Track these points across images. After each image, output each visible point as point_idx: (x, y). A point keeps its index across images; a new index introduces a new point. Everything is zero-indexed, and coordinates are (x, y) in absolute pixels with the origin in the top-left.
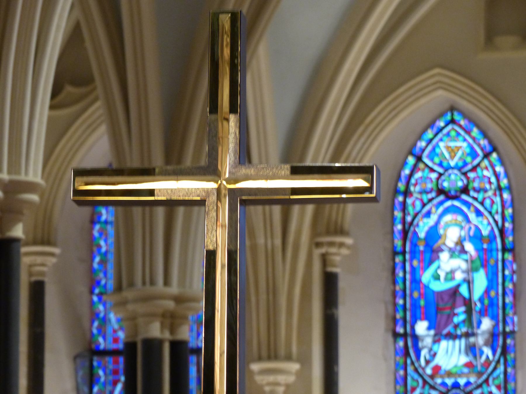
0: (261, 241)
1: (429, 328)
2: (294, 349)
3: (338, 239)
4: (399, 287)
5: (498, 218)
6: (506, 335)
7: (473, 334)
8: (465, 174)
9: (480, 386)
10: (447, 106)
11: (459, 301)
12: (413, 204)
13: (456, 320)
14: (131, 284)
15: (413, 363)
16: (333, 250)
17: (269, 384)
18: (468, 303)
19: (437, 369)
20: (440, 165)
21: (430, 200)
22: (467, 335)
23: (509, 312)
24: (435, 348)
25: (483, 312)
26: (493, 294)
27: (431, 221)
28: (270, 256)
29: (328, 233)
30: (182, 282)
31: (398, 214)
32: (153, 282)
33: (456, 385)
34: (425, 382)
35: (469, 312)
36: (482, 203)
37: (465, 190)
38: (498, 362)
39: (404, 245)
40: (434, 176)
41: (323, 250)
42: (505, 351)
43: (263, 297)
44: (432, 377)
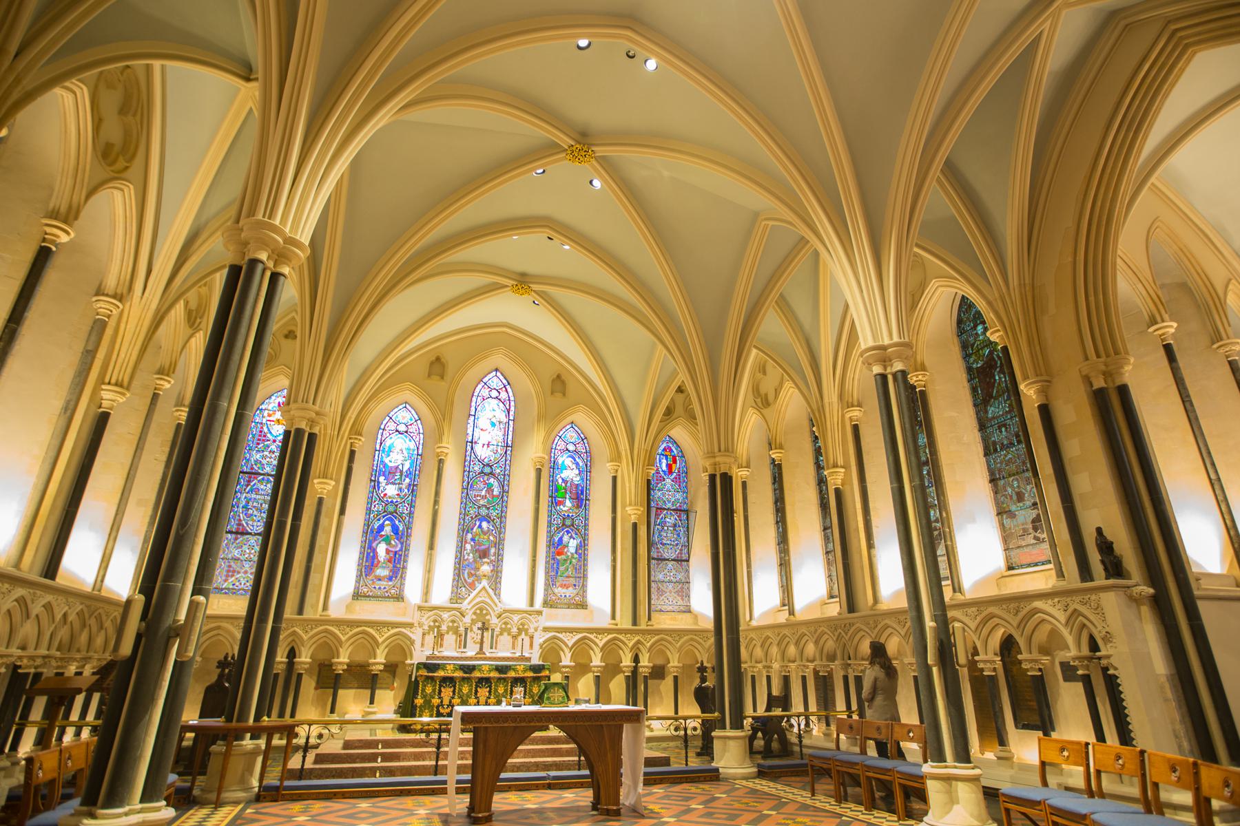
0: (329, 431)
3: (359, 437)
4: (375, 463)
6: (414, 485)
14: (296, 401)
18: (401, 472)
19: (385, 495)
23: (417, 477)
25: (407, 476)
29: (355, 434)
30: (321, 407)
33: (392, 502)
35: (401, 475)
37: (406, 432)
42: (413, 491)
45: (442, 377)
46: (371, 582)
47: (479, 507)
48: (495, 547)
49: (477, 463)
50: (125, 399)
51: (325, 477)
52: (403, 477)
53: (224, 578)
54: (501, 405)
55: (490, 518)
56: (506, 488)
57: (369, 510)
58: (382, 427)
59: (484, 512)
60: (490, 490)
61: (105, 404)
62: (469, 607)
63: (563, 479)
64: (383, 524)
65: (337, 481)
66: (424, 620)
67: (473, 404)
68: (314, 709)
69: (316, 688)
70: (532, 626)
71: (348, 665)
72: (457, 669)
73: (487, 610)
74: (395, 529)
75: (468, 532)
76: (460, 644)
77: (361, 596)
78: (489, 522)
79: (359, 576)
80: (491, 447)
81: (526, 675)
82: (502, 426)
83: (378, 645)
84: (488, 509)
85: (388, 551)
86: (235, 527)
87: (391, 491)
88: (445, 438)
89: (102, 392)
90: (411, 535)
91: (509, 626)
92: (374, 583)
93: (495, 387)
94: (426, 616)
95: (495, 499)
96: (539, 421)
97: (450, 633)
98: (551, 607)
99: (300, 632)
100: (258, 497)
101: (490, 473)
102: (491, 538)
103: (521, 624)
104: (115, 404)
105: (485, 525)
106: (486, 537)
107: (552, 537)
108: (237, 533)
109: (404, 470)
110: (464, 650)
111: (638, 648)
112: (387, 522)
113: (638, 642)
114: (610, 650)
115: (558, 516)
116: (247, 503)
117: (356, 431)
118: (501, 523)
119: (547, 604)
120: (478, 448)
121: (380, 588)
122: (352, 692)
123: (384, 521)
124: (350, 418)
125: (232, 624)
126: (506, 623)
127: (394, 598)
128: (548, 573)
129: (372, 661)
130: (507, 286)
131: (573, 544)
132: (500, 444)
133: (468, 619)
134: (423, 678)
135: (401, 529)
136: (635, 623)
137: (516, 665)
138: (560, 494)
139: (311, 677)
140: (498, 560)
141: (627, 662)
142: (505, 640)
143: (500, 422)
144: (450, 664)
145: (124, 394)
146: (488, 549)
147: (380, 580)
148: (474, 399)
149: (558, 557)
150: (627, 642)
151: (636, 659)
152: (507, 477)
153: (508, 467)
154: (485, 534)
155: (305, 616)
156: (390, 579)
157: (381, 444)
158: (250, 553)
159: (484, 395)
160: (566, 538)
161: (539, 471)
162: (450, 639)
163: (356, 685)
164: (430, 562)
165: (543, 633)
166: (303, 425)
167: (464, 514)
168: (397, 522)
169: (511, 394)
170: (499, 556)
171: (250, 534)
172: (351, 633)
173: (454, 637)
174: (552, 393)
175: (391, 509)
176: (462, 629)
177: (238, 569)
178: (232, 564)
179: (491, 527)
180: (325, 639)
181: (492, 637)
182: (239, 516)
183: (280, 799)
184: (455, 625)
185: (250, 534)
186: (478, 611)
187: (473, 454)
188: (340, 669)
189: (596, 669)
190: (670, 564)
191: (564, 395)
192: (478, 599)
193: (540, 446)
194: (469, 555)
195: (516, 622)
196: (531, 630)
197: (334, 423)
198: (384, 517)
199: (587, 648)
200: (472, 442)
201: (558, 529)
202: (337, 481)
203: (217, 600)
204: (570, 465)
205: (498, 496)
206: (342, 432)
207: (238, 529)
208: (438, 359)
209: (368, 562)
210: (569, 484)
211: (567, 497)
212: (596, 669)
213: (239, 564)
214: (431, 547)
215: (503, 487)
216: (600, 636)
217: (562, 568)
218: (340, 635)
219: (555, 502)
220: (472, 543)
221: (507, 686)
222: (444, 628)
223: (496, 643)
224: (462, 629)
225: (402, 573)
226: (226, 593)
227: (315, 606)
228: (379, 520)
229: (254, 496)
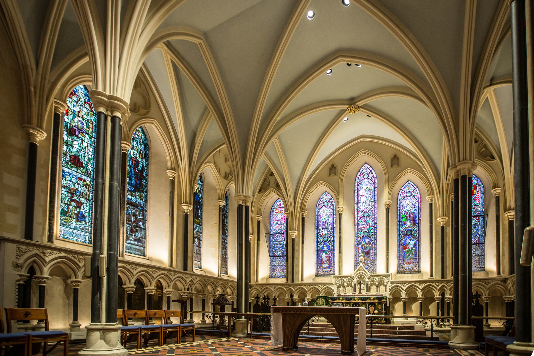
0: (290, 211)
2: (297, 229)
6: (334, 228)
11: (326, 223)
16: (303, 213)
18: (328, 223)
19: (323, 234)
22: (328, 228)
28: (292, 213)
29: (303, 210)
31: (317, 210)
35: (328, 225)
37: (328, 205)
48: (373, 249)
49: (361, 212)
55: (369, 237)
57: (317, 242)
58: (317, 205)
59: (366, 234)
63: (405, 212)
64: (323, 246)
65: (298, 231)
74: (328, 248)
75: (359, 244)
76: (353, 290)
78: (369, 239)
84: (368, 232)
85: (326, 257)
91: (375, 282)
95: (371, 228)
97: (349, 286)
99: (292, 289)
100: (278, 242)
101: (368, 216)
102: (370, 246)
105: (367, 240)
106: (368, 246)
107: (400, 241)
108: (273, 256)
110: (355, 293)
111: (444, 289)
113: (443, 286)
114: (428, 291)
117: (303, 208)
123: (324, 245)
124: (298, 203)
126: (373, 281)
131: (412, 243)
136: (443, 276)
138: (404, 219)
141: (437, 295)
142: (374, 288)
146: (369, 250)
150: (437, 287)
151: (443, 294)
152: (376, 216)
153: (376, 211)
154: (367, 244)
157: (318, 212)
160: (408, 241)
162: (349, 289)
164: (340, 259)
167: (357, 237)
171: (277, 256)
173: (351, 288)
175: (326, 239)
179: (370, 241)
180: (301, 291)
184: (350, 283)
185: (277, 256)
187: (358, 209)
189: (419, 299)
195: (377, 280)
196: (385, 283)
198: (323, 243)
199: (414, 290)
201: (403, 237)
202: (298, 231)
205: (372, 226)
206: (296, 210)
209: (320, 263)
210: (408, 214)
211: (408, 220)
212: (419, 299)
214: (340, 252)
216: (421, 285)
217: (406, 255)
218: (306, 289)
219: (400, 223)
220: (362, 249)
222: (345, 284)
223: (369, 289)
229: (276, 242)
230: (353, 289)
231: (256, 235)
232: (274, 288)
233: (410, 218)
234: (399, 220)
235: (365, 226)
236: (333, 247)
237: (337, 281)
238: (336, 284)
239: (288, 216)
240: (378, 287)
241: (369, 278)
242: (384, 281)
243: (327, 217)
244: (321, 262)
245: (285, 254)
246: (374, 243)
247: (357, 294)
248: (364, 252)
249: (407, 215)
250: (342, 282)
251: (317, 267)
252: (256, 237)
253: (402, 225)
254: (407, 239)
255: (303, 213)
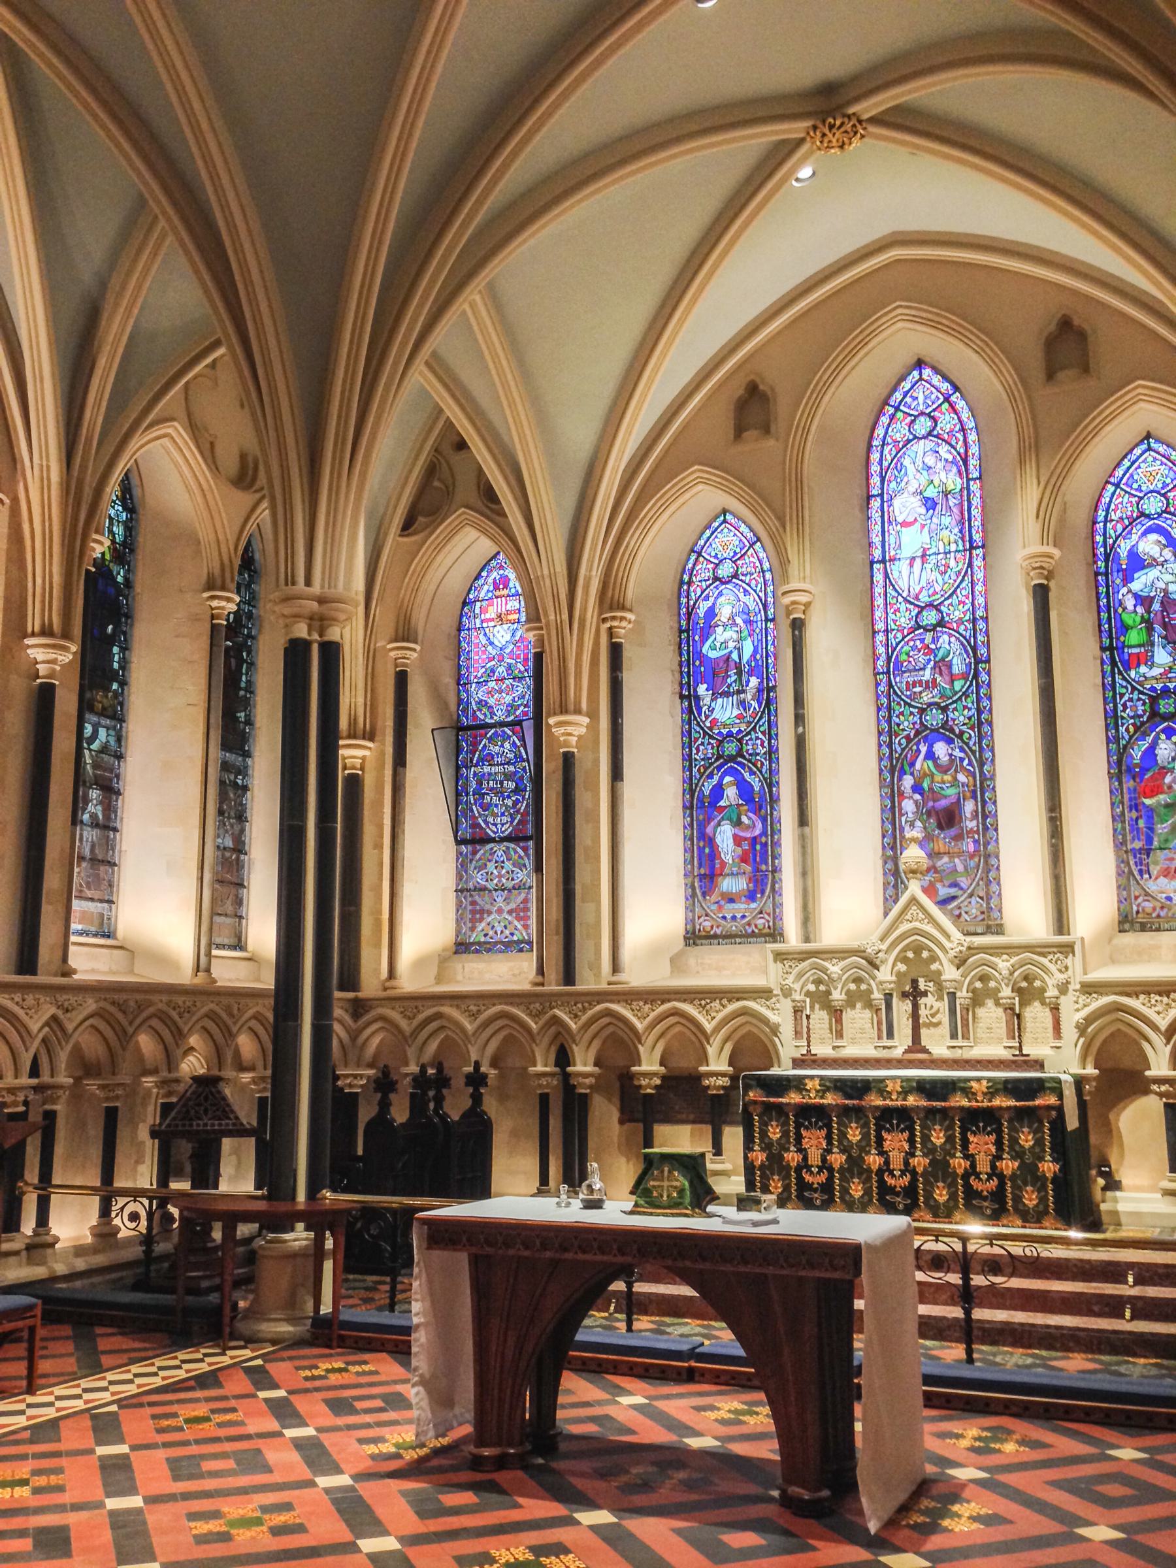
0: (552, 617)
1: (707, 690)
2: (584, 706)
5: (762, 595)
6: (769, 690)
7: (743, 691)
8: (734, 562)
9: (749, 733)
10: (719, 509)
11: (732, 665)
12: (695, 591)
13: (729, 681)
15: (695, 718)
16: (615, 623)
17: (563, 734)
18: (739, 667)
19: (714, 721)
20: (716, 557)
21: (708, 587)
24: (713, 705)
25: (751, 673)
26: (758, 657)
27: (709, 603)
29: (611, 609)
32: (293, 584)
33: (730, 734)
34: (705, 733)
35: (739, 674)
36: (748, 585)
37: (735, 576)
38: (763, 712)
39: (688, 624)
40: (711, 566)
41: (608, 625)
43: (556, 663)
44: (711, 729)
45: (766, 430)
46: (714, 907)
47: (922, 711)
48: (974, 797)
49: (903, 607)
50: (71, 657)
51: (564, 710)
52: (745, 677)
53: (470, 925)
54: (944, 449)
55: (952, 731)
56: (983, 651)
57: (688, 759)
59: (934, 718)
60: (942, 666)
61: (42, 669)
62: (884, 947)
63: (1136, 596)
65: (593, 714)
66: (790, 980)
67: (875, 468)
68: (623, 1160)
69: (621, 1122)
70: (1050, 982)
71: (664, 1078)
72: (828, 1089)
73: (930, 950)
74: (745, 790)
75: (902, 772)
76: (879, 1029)
77: (701, 938)
78: (949, 741)
79: (691, 897)
80: (932, 560)
81: (997, 1102)
82: (952, 502)
83: (704, 1036)
84: (944, 709)
85: (738, 840)
86: (469, 830)
87: (725, 712)
88: (793, 569)
89: (29, 651)
90: (778, 799)
91: (992, 984)
92: (720, 908)
93: (921, 407)
94: (795, 971)
95: (958, 685)
96: (1022, 462)
97: (859, 1005)
98: (1143, 928)
99: (566, 1018)
100: (494, 769)
102: (962, 778)
103: (1026, 978)
104: (58, 668)
105: (941, 749)
106: (948, 778)
107: (1123, 752)
109: (745, 660)
110: (889, 1043)
112: (727, 779)
115: (1135, 696)
116: (479, 783)
118: (981, 737)
119: (1132, 923)
120: (899, 571)
121: (734, 918)
122: (687, 1129)
125: (458, 1007)
126: (983, 978)
127: (765, 935)
128: (1124, 843)
129: (703, 1069)
130: (801, 141)
132: (953, 547)
133: (885, 974)
134: (759, 1109)
135: (757, 788)
137: (968, 1080)
138: (1134, 637)
139: (610, 1100)
140: (986, 829)
142: (991, 1016)
143: (946, 494)
144: (812, 1077)
145: (65, 649)
147: (731, 901)
148: (875, 456)
149: (1148, 802)
152: (981, 625)
154: (944, 770)
155: (579, 988)
156: (751, 897)
158: (500, 876)
159: (898, 437)
161: (1041, 595)
162: (858, 1019)
163: (692, 1117)
165: (1083, 999)
166: (301, 631)
167: (887, 732)
168: (747, 775)
169: (965, 415)
170: (985, 817)
171: (493, 840)
172: (652, 1015)
173: (867, 1014)
174: (1050, 375)
175: (730, 748)
176: (877, 995)
177: (487, 907)
178: (477, 898)
180: (611, 1029)
181: (952, 1011)
182: (472, 811)
183: (335, 1344)
184: (863, 987)
185: (493, 840)
186: (910, 955)
187: (890, 590)
188: (649, 1086)
190: (499, 850)
191: (1086, 369)
192: (905, 927)
193: (1033, 528)
194: (912, 825)
195: (1005, 972)
196: (1051, 992)
197: (556, 597)
198: (719, 768)
200: (883, 561)
201: (1137, 729)
202: (593, 714)
203: (460, 966)
204: (1155, 551)
205: (964, 676)
207: (473, 834)
208: (753, 390)
210: (1156, 606)
213: (487, 898)
214: (803, 820)
215: (974, 649)
220: (917, 797)
221: (951, 1127)
222: (837, 995)
223: (965, 1025)
224: (877, 995)
225: (774, 883)
226: (477, 951)
227: (595, 966)
228: (711, 776)
229: (487, 769)
230: (879, 1023)
231: (389, 739)
232: (474, 1016)
233: (1165, 628)
234: (1106, 642)
235: (927, 675)
236: (770, 786)
237: (791, 978)
238: (787, 992)
239: (541, 641)
240: (1016, 1019)
241: (960, 962)
242: (1043, 981)
243: (735, 636)
244: (713, 867)
245: (530, 829)
246: (982, 764)
247: (898, 1053)
248: (929, 814)
249: (1149, 612)
250: (818, 982)
251: (694, 895)
252: (389, 750)
253: (1128, 668)
254: (1157, 738)
255: (615, 623)
